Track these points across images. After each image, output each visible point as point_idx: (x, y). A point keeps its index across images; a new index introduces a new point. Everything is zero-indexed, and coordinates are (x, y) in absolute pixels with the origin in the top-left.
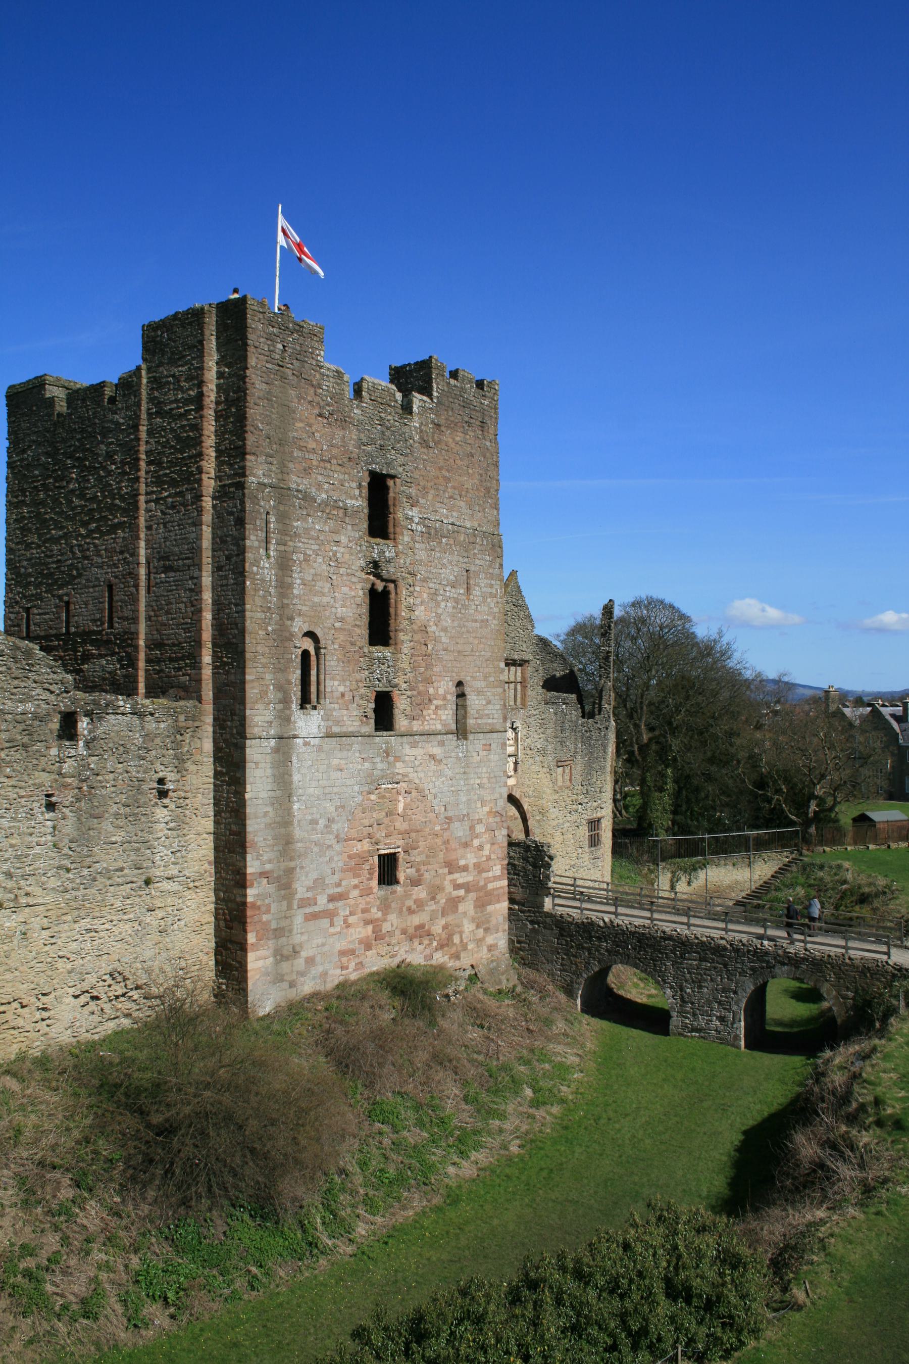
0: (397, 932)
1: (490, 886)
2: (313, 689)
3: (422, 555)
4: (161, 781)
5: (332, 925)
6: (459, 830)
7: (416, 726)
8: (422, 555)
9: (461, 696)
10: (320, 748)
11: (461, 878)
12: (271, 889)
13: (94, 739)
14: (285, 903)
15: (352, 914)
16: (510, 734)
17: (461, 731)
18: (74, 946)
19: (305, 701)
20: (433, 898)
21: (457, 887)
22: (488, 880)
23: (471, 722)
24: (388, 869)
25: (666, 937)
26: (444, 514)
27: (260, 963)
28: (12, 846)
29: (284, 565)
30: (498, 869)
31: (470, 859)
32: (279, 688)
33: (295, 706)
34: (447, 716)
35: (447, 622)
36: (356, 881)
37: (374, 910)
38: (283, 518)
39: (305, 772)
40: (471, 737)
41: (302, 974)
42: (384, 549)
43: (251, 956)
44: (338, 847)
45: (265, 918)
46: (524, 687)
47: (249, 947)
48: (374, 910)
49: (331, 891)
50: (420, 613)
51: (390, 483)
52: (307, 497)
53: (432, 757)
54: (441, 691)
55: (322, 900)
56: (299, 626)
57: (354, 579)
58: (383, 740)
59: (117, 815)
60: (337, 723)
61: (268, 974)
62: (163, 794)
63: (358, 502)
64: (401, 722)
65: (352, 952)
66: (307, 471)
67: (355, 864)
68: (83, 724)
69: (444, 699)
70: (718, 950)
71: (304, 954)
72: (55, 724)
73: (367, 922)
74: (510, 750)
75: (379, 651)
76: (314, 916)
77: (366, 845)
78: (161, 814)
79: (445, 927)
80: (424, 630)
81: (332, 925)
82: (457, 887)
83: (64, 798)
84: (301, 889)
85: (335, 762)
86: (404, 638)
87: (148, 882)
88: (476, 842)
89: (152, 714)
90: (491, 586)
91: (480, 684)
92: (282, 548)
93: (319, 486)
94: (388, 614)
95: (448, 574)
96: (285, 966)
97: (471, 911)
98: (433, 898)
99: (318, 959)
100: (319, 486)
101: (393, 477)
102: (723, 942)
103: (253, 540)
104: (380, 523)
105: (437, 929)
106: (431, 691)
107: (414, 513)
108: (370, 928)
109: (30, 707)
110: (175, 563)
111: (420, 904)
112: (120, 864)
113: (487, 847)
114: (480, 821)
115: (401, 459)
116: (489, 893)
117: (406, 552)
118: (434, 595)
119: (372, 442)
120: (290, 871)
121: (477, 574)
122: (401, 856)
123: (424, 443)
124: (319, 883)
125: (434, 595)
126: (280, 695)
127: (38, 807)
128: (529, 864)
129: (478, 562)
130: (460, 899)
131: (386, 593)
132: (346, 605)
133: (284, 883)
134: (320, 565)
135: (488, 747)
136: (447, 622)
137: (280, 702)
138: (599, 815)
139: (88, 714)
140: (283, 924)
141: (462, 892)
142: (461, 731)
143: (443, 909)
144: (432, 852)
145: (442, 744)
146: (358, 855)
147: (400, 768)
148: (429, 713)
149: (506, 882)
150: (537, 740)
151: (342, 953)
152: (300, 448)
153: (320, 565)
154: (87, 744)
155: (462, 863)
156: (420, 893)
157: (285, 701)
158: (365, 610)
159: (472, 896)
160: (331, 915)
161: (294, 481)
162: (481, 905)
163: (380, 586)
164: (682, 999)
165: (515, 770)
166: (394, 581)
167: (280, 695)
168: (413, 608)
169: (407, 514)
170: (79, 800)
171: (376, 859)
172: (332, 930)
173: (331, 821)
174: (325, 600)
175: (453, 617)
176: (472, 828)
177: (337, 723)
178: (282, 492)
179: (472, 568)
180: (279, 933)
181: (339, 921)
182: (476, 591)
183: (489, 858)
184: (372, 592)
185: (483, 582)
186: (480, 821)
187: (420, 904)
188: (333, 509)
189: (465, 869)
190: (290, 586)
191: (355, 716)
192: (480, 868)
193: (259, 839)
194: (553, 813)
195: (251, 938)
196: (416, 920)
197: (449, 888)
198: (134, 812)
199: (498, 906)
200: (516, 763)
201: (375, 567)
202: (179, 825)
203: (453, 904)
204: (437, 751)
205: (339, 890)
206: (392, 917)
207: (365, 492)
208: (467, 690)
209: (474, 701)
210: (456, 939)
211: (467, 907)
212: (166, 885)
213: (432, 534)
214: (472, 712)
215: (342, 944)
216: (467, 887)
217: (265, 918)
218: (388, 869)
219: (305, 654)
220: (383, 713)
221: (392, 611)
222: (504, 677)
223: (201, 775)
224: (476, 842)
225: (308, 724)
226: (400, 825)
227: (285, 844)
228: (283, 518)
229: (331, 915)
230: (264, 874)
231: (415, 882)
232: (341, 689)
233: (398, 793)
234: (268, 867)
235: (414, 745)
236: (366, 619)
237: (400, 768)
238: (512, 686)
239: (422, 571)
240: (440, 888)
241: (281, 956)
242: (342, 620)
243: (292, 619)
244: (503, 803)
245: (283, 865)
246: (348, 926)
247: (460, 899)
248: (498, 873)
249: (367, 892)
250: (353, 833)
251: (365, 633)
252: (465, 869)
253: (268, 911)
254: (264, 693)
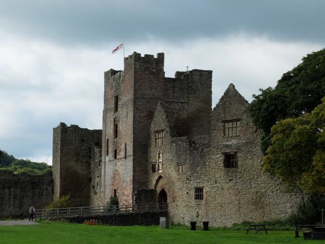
21: (124, 200)
58: (116, 161)
64: (118, 157)
123: (122, 83)
136: (124, 128)
138: (201, 185)
168: (120, 127)
186: (128, 182)
204: (122, 163)
209: (128, 148)
214: (127, 151)
225: (107, 159)
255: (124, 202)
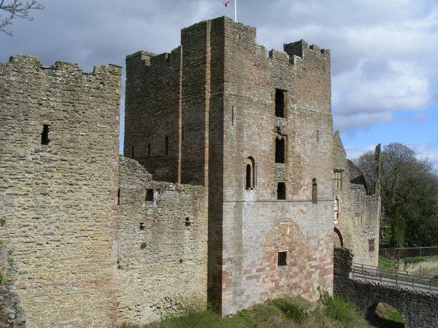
0: (286, 286)
1: (326, 267)
2: (252, 181)
3: (298, 124)
4: (187, 219)
5: (258, 281)
6: (313, 243)
7: (295, 197)
8: (298, 124)
9: (315, 185)
10: (254, 207)
11: (313, 263)
12: (232, 265)
13: (160, 201)
14: (238, 272)
15: (266, 277)
16: (335, 202)
17: (315, 200)
18: (151, 286)
19: (248, 186)
20: (301, 272)
21: (312, 267)
22: (325, 265)
23: (319, 196)
24: (282, 258)
25: (403, 291)
26: (308, 107)
27: (227, 297)
28: (126, 244)
29: (240, 128)
30: (329, 260)
31: (317, 255)
32: (237, 180)
33: (244, 188)
34: (309, 193)
35: (309, 153)
36: (268, 264)
37: (276, 276)
38: (239, 109)
39: (248, 216)
40: (319, 202)
41: (244, 302)
42: (281, 122)
43: (223, 293)
44: (261, 249)
45: (230, 277)
46: (341, 181)
47: (223, 290)
48: (276, 276)
49: (258, 267)
50: (297, 149)
51: (285, 93)
52: (250, 100)
53: (302, 211)
54: (306, 183)
55: (254, 272)
56: (246, 154)
57: (269, 135)
58: (281, 203)
59: (169, 233)
60: (262, 196)
61: (230, 302)
62: (188, 224)
63: (271, 102)
64: (289, 196)
65: (266, 293)
66: (249, 89)
67: (268, 257)
68: (156, 194)
69: (308, 186)
70: (426, 298)
71: (246, 293)
72: (144, 194)
73: (273, 281)
74: (335, 209)
75: (279, 165)
76: (251, 278)
77: (273, 248)
78: (187, 233)
79: (306, 284)
80: (299, 156)
81: (258, 281)
82: (312, 267)
83: (148, 225)
84: (245, 266)
85: (260, 212)
86: (291, 160)
87: (181, 261)
88: (320, 248)
89: (184, 191)
90: (328, 138)
91: (322, 180)
92: (239, 121)
93: (254, 95)
94: (284, 149)
95: (309, 132)
96: (238, 299)
97: (318, 278)
98: (301, 272)
99: (252, 296)
100: (254, 95)
101: (286, 91)
102: (429, 294)
103: (227, 118)
104: (280, 110)
105: (303, 285)
106: (302, 182)
107: (295, 106)
108: (274, 283)
109: (134, 187)
110: (194, 127)
111: (296, 274)
112: (170, 253)
113: (325, 250)
114: (322, 239)
115: (289, 84)
116: (325, 270)
117: (291, 123)
118: (303, 142)
119: (277, 76)
120: (240, 258)
121: (322, 133)
122: (288, 253)
124: (253, 264)
125: (303, 142)
126: (237, 184)
127: (137, 229)
128: (343, 258)
129: (322, 127)
130: (313, 272)
131: (283, 140)
132: (265, 145)
133: (238, 263)
134: (255, 129)
135: (326, 207)
136: (309, 153)
137: (237, 186)
139: (158, 190)
140: (237, 280)
141: (314, 269)
142: (315, 200)
143: (306, 276)
144: (301, 251)
145: (306, 205)
146: (270, 253)
147: (288, 215)
148: (300, 192)
149: (333, 266)
150: (347, 204)
151: (262, 294)
152: (247, 79)
153: (255, 129)
154: (157, 203)
155: (314, 257)
156: (296, 269)
157: (240, 186)
158: (274, 146)
159: (318, 271)
160: (257, 277)
161: (244, 93)
162: (322, 275)
163: (280, 137)
164: (410, 319)
165: (337, 217)
166: (286, 135)
167: (237, 184)
168: (295, 147)
169: (292, 106)
170: (153, 226)
171: (277, 254)
172: (258, 284)
173: (258, 237)
174: (257, 143)
175: (311, 151)
176: (318, 242)
177: (262, 196)
178: (239, 97)
179: (320, 130)
180: (235, 284)
181: (261, 280)
182: (321, 140)
183: (326, 255)
184: (277, 140)
185: (324, 136)
186: (322, 239)
187: (296, 274)
188: (261, 105)
189: (315, 259)
190: (242, 137)
191: (269, 193)
192: (322, 259)
193: (228, 244)
194: (353, 236)
195: (224, 286)
196: (294, 281)
197: (308, 268)
198: (176, 232)
199: (329, 276)
200: (338, 214)
201: (278, 130)
202: (194, 237)
203: (310, 274)
204: (304, 209)
205: (261, 267)
206: (284, 279)
207: (274, 97)
208: (317, 182)
209: (319, 187)
210: (311, 290)
211: (316, 276)
212: (189, 263)
213: (302, 115)
214: (319, 192)
215: (261, 290)
216: (316, 267)
217: (230, 277)
218: (282, 258)
219: (248, 166)
220: (281, 192)
221: (285, 148)
222: (333, 177)
223: (203, 218)
224: (320, 248)
225: (249, 196)
226: (288, 240)
227: (239, 247)
228: (239, 109)
229: (257, 277)
230: (230, 259)
231: (294, 265)
232: (263, 181)
233: (287, 226)
234: (231, 256)
235: (294, 206)
236: (274, 152)
237: (288, 215)
238: (336, 181)
239: (298, 131)
240: (304, 267)
241: (236, 294)
242: (264, 152)
243: (243, 151)
244: (332, 231)
245: (238, 256)
246: (265, 282)
247: (313, 272)
248: (330, 261)
249: (273, 268)
250: (268, 243)
251: (274, 157)
252: (315, 259)
253: (231, 275)
254: (231, 183)
255: (311, 270)
